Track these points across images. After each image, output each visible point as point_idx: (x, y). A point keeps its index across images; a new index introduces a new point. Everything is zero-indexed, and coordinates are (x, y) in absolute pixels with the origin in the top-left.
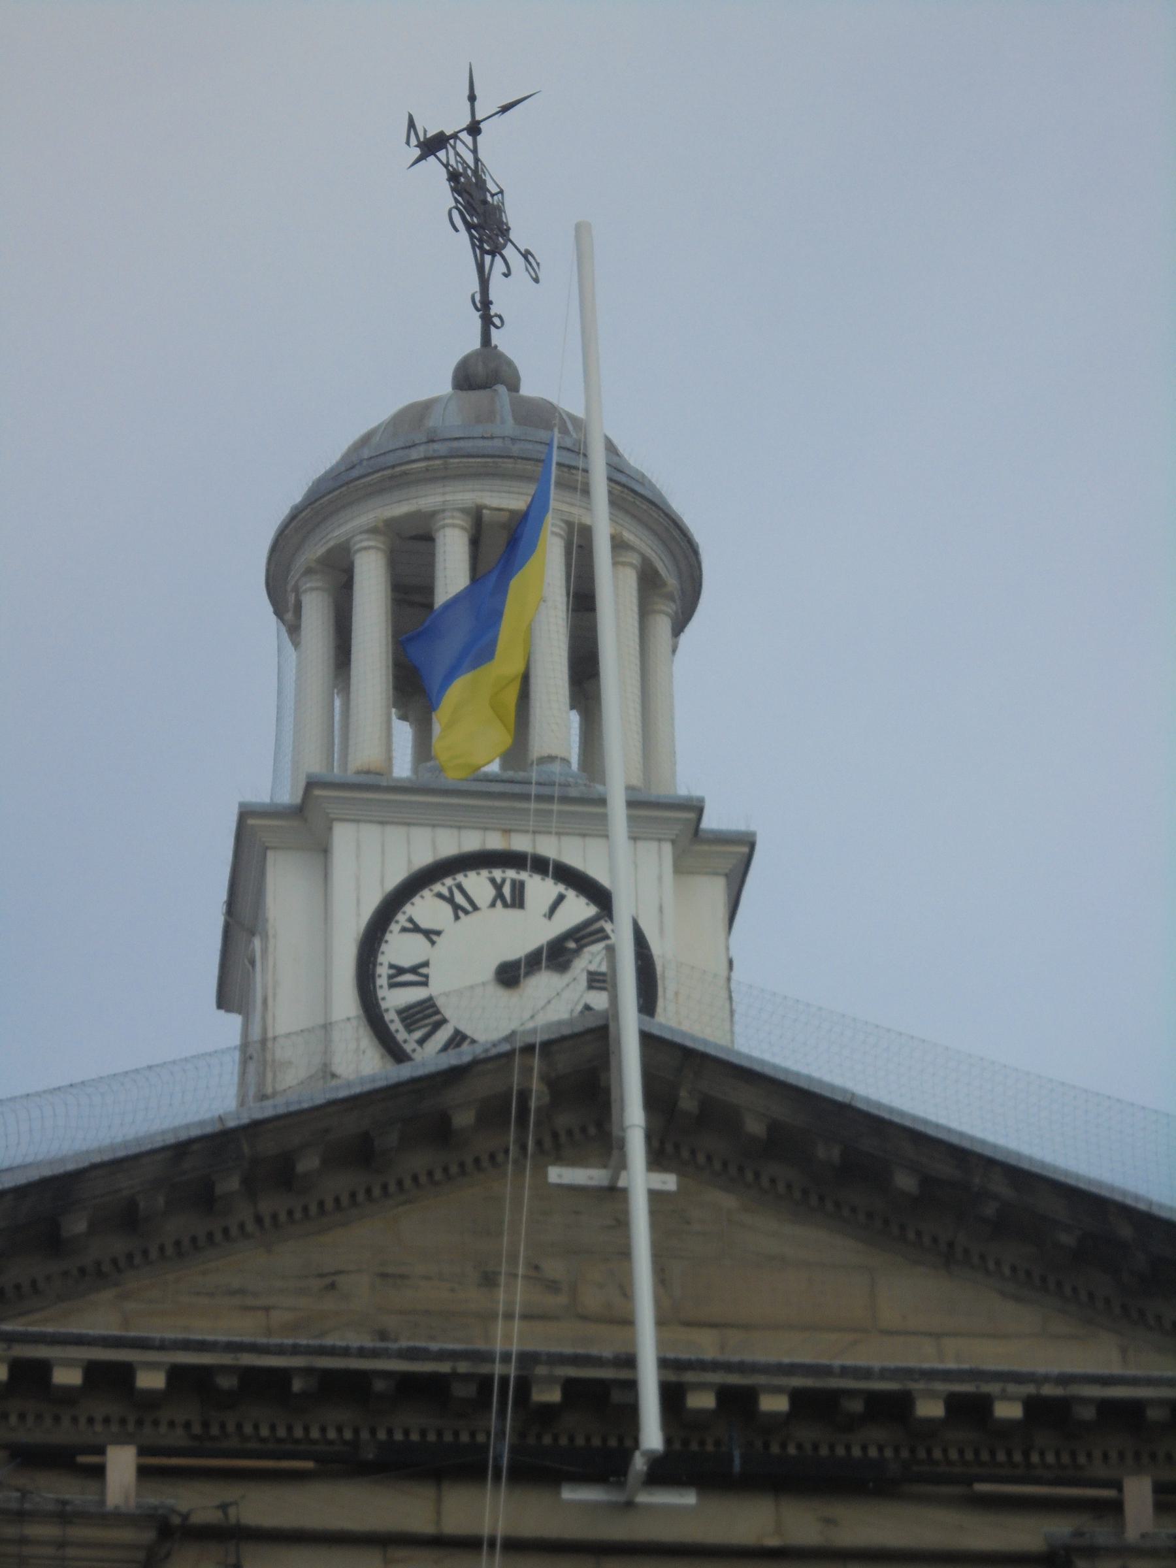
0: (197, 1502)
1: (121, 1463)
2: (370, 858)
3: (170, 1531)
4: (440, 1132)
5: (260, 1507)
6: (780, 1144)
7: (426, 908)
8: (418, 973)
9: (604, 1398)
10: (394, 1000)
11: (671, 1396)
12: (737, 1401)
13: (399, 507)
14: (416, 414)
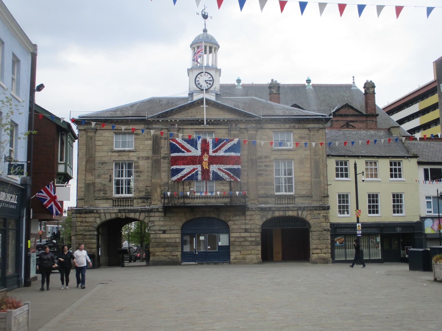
0: (181, 127)
1: (177, 125)
2: (196, 72)
3: (180, 129)
4: (194, 105)
5: (184, 127)
6: (214, 104)
7: (199, 76)
8: (198, 81)
9: (203, 121)
10: (197, 83)
11: (207, 120)
12: (211, 121)
13: (198, 45)
14: (199, 37)
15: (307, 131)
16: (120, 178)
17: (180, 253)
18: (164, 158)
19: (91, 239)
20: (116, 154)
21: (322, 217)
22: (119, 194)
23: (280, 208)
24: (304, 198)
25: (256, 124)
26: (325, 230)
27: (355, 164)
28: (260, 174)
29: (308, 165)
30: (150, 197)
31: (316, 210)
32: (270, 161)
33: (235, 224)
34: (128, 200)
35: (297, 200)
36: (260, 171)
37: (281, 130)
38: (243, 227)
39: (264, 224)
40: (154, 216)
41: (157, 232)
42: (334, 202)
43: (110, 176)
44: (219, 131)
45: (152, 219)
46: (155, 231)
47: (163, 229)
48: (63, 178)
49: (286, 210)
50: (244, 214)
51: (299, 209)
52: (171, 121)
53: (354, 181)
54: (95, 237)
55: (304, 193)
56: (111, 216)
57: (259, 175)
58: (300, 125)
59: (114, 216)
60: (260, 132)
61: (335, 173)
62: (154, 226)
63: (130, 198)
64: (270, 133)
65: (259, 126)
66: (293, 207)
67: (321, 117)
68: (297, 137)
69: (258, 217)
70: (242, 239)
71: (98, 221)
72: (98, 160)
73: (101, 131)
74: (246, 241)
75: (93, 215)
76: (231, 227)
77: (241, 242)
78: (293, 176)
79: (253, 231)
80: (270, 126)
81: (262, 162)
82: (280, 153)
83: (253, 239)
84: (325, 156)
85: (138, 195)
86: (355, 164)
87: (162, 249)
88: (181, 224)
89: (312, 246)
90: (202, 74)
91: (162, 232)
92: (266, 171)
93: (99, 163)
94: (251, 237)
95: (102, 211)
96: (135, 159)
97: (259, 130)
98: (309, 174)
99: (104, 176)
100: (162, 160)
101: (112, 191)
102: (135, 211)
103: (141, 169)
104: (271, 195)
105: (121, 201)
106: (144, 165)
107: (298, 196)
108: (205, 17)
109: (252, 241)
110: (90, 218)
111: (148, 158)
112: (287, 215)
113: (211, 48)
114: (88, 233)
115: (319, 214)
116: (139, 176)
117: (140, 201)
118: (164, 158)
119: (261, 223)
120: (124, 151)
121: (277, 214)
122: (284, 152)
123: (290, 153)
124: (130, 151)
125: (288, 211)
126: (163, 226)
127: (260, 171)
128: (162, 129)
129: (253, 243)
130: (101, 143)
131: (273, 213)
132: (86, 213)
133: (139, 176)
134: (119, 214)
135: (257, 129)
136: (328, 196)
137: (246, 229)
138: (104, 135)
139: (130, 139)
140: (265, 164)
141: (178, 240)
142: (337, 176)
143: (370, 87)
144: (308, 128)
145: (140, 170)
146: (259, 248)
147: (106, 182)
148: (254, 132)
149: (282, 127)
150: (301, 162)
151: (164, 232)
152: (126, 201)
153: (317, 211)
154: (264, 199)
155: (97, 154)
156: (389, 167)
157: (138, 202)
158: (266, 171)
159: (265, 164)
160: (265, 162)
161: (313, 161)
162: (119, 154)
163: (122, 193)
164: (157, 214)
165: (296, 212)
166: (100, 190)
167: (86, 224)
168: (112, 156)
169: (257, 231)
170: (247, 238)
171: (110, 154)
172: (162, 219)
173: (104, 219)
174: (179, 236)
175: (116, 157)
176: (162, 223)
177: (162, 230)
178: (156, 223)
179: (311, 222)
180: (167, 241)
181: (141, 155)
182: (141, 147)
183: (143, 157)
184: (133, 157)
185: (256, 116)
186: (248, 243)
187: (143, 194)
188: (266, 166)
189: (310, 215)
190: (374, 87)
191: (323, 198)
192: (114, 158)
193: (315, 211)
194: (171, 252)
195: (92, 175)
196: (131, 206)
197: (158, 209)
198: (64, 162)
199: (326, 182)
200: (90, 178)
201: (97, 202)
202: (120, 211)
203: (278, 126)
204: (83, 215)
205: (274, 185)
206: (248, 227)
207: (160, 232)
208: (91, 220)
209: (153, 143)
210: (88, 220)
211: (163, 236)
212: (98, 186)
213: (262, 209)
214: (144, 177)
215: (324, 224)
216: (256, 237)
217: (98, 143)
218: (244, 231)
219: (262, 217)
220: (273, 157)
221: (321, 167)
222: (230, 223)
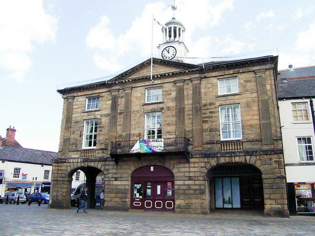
2: (163, 47)
15: (252, 75)
17: (130, 199)
18: (120, 113)
20: (86, 114)
25: (200, 74)
28: (205, 121)
29: (256, 108)
31: (267, 155)
32: (215, 108)
33: (179, 172)
35: (245, 144)
36: (205, 118)
37: (226, 76)
38: (187, 174)
40: (109, 165)
41: (111, 179)
44: (166, 85)
45: (107, 167)
47: (115, 176)
49: (231, 156)
50: (188, 162)
55: (252, 137)
57: (204, 122)
58: (244, 69)
60: (204, 82)
64: (214, 80)
66: (240, 152)
68: (242, 82)
70: (185, 187)
71: (69, 169)
72: (74, 120)
73: (77, 97)
74: (190, 189)
76: (175, 175)
77: (184, 190)
79: (196, 179)
80: (214, 74)
81: (208, 109)
82: (224, 99)
83: (197, 187)
87: (114, 195)
89: (266, 196)
91: (114, 179)
92: (211, 117)
96: (99, 117)
97: (204, 79)
98: (257, 117)
99: (76, 133)
104: (217, 141)
106: (105, 121)
108: (174, 8)
109: (195, 190)
111: (108, 115)
114: (61, 179)
115: (271, 159)
116: (101, 131)
117: (101, 151)
118: (120, 113)
119: (206, 171)
120: (92, 111)
121: (222, 160)
122: (229, 98)
123: (236, 97)
124: (96, 111)
125: (235, 157)
126: (116, 174)
127: (205, 118)
128: (119, 89)
129: (197, 192)
130: (76, 107)
131: (218, 160)
133: (101, 131)
134: (83, 163)
135: (201, 79)
137: (189, 177)
140: (210, 110)
141: (128, 187)
147: (77, 137)
148: (199, 82)
149: (226, 73)
150: (248, 105)
151: (116, 179)
153: (268, 156)
155: (74, 116)
157: (99, 153)
158: (211, 117)
159: (210, 110)
160: (210, 109)
161: (260, 104)
162: (88, 114)
165: (243, 157)
166: (73, 144)
168: (83, 116)
172: (115, 167)
174: (129, 183)
176: (114, 171)
178: (110, 171)
180: (118, 187)
181: (103, 113)
182: (104, 107)
183: (104, 115)
186: (192, 192)
187: (103, 147)
188: (211, 112)
189: (259, 161)
191: (275, 142)
192: (84, 118)
194: (121, 198)
199: (278, 124)
200: (67, 134)
201: (70, 153)
203: (221, 73)
204: (60, 165)
206: (192, 174)
208: (64, 168)
209: (112, 102)
212: (72, 141)
214: (105, 131)
215: (277, 170)
217: (74, 107)
218: (187, 178)
220: (217, 104)
221: (270, 108)
222: (175, 171)
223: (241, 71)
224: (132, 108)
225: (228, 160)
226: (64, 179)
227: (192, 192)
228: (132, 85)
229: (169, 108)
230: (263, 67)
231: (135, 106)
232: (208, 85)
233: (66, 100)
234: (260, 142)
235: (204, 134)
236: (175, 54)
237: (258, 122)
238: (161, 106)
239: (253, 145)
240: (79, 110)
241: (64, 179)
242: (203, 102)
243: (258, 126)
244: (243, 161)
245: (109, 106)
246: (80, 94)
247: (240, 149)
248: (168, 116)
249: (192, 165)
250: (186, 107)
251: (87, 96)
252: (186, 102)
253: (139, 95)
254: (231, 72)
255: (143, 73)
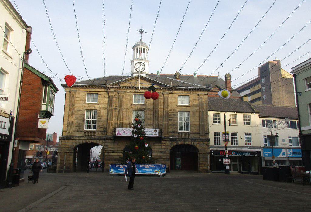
7: (137, 64)
10: (136, 68)
16: (89, 120)
18: (115, 108)
19: (69, 155)
20: (87, 106)
21: (205, 146)
22: (88, 129)
23: (181, 139)
24: (196, 134)
26: (207, 153)
27: (225, 115)
29: (198, 115)
30: (106, 131)
32: (176, 112)
33: (155, 148)
34: (93, 133)
35: (191, 135)
37: (183, 95)
38: (160, 150)
39: (172, 149)
40: (108, 142)
42: (212, 137)
43: (83, 118)
46: (108, 151)
48: (44, 114)
50: (160, 143)
51: (193, 140)
52: (120, 87)
53: (224, 125)
54: (73, 154)
55: (195, 131)
56: (82, 141)
57: (170, 120)
58: (193, 92)
59: (84, 142)
60: (170, 96)
61: (212, 120)
62: (108, 148)
63: (94, 131)
64: (176, 96)
65: (170, 92)
67: (205, 88)
69: (169, 144)
72: (76, 108)
73: (79, 92)
75: (71, 141)
78: (189, 121)
79: (165, 152)
83: (166, 157)
84: (207, 110)
85: (99, 130)
86: (225, 115)
88: (123, 147)
90: (139, 63)
92: (173, 118)
93: (77, 110)
94: (164, 156)
95: (77, 138)
96: (98, 109)
97: (170, 94)
98: (198, 120)
100: (114, 110)
101: (84, 127)
102: (97, 139)
103: (102, 114)
104: (176, 132)
105: (89, 133)
107: (191, 133)
108: (141, 32)
109: (164, 159)
110: (70, 143)
111: (105, 108)
112: (185, 144)
113: (144, 49)
114: (68, 152)
115: (204, 144)
119: (170, 148)
120: (92, 104)
121: (179, 143)
124: (95, 104)
125: (186, 141)
127: (170, 117)
131: (177, 142)
132: (67, 139)
133: (100, 119)
136: (209, 133)
138: (81, 95)
139: (95, 97)
142: (214, 122)
143: (228, 76)
144: (198, 95)
145: (101, 115)
146: (169, 162)
150: (194, 113)
151: (113, 152)
152: (92, 133)
153: (203, 142)
154: (172, 134)
155: (76, 105)
156: (243, 118)
158: (173, 118)
159: (173, 114)
162: (89, 105)
163: (90, 128)
164: (110, 141)
165: (190, 142)
167: (66, 146)
169: (167, 152)
170: (162, 157)
171: (84, 105)
172: (112, 144)
173: (78, 144)
175: (87, 107)
176: (112, 147)
177: (112, 151)
178: (109, 147)
179: (199, 148)
180: (115, 157)
182: (102, 102)
183: (103, 108)
184: (97, 107)
185: (169, 86)
186: (162, 160)
187: (102, 130)
188: (173, 115)
189: (198, 144)
190: (230, 76)
191: (206, 134)
192: (86, 108)
193: (201, 142)
195: (72, 117)
196: (95, 136)
197: (110, 138)
198: (46, 103)
202: (88, 139)
204: (66, 141)
205: (178, 126)
206: (163, 150)
207: (111, 152)
208: (71, 143)
210: (68, 144)
211: (113, 154)
213: (171, 140)
216: (167, 156)
217: (76, 99)
218: (160, 152)
219: (171, 144)
220: (178, 110)
223: (191, 93)
224: (124, 106)
225: (182, 143)
226: (70, 151)
227: (162, 160)
228: (124, 90)
229: (149, 109)
230: (205, 93)
231: (126, 106)
232: (173, 99)
233: (68, 92)
234: (199, 134)
235: (170, 127)
236: (144, 68)
237: (198, 123)
238: (144, 107)
239: (196, 135)
240: (81, 102)
241: (70, 151)
242: (170, 108)
243: (198, 125)
244: (190, 144)
245: (107, 102)
246: (81, 89)
247: (188, 137)
248: (148, 114)
249: (162, 145)
250: (160, 110)
251: (88, 92)
252: (160, 107)
253: (129, 98)
254: (186, 92)
255: (133, 83)
